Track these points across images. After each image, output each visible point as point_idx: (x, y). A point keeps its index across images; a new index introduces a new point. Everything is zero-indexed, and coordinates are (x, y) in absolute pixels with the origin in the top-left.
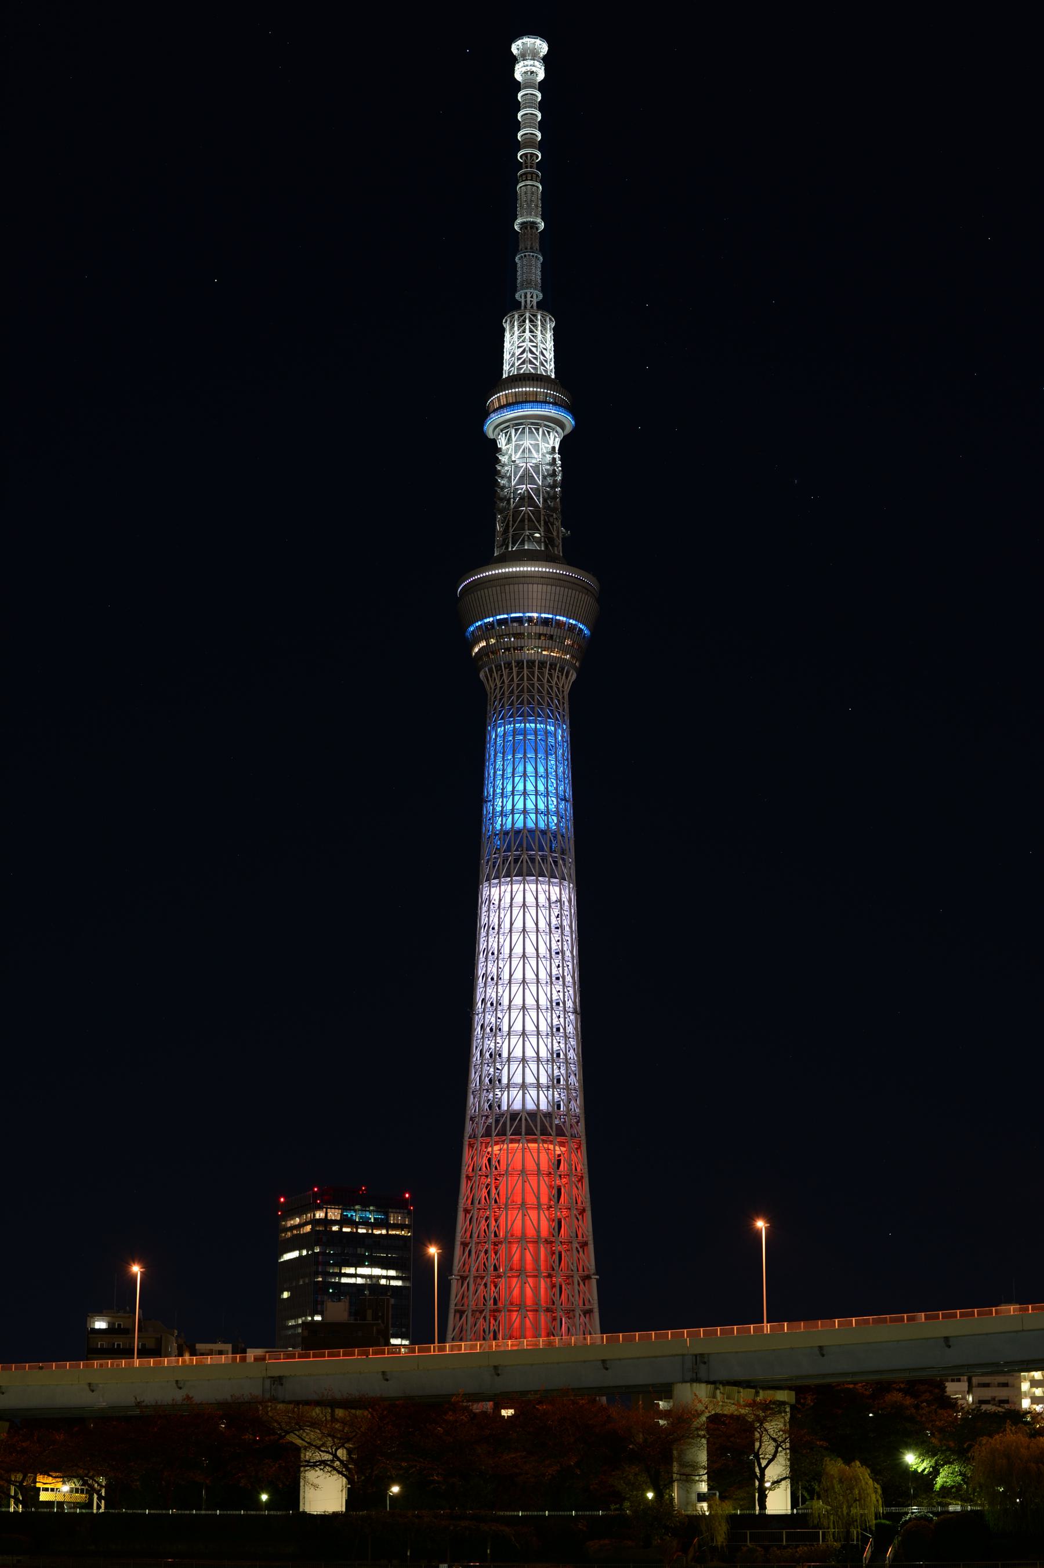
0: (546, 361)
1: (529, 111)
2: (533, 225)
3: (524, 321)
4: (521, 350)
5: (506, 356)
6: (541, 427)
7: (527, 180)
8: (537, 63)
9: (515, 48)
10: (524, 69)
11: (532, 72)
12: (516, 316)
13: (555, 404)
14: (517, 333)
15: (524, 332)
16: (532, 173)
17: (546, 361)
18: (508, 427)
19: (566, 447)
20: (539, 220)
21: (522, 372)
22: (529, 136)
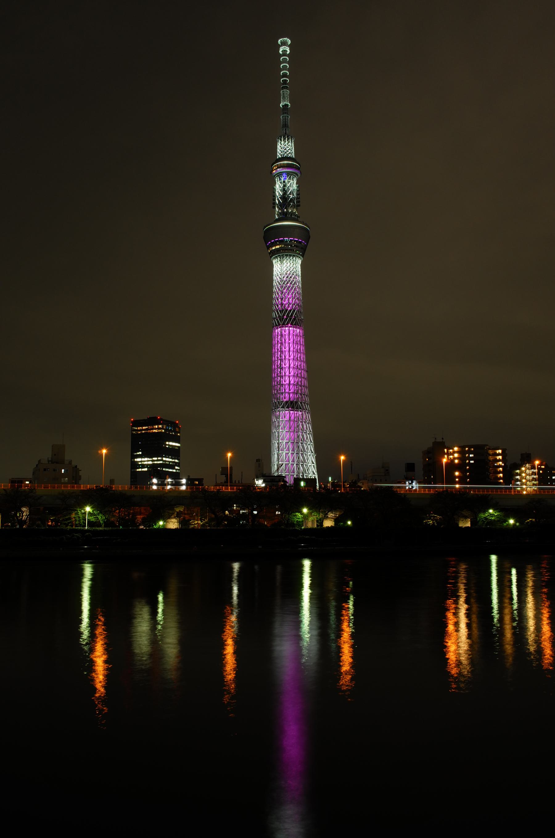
0: (292, 153)
2: (286, 105)
3: (285, 139)
5: (278, 151)
6: (292, 175)
7: (283, 89)
8: (287, 47)
9: (279, 41)
10: (283, 49)
11: (285, 50)
13: (296, 168)
14: (282, 142)
15: (285, 142)
16: (285, 87)
17: (292, 153)
20: (289, 104)
21: (284, 156)
22: (284, 73)
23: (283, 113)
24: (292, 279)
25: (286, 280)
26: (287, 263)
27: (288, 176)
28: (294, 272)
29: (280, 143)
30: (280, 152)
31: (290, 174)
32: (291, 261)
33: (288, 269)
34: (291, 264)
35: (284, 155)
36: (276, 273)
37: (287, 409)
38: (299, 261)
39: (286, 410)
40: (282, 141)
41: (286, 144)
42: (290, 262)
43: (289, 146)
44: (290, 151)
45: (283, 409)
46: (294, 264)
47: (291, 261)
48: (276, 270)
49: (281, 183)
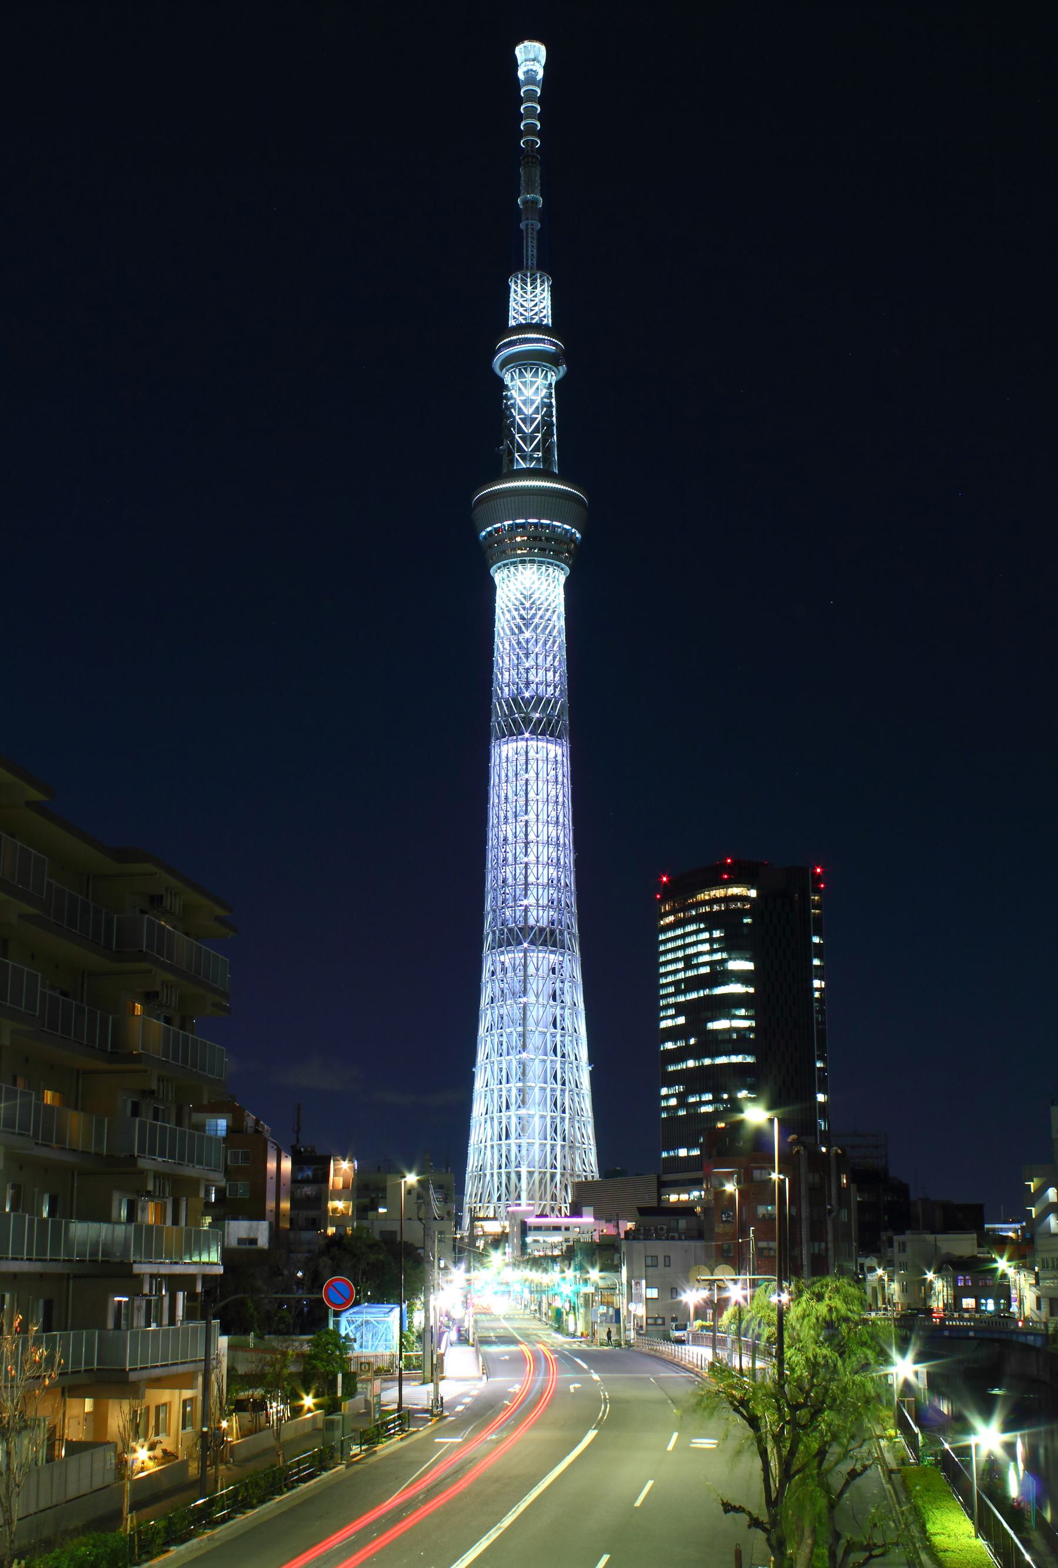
1: (530, 104)
2: (535, 202)
4: (533, 303)
12: (529, 274)
14: (529, 288)
15: (536, 288)
18: (526, 364)
19: (561, 388)
21: (534, 321)
23: (527, 219)
26: (540, 581)
27: (543, 370)
28: (556, 607)
29: (522, 288)
30: (521, 310)
31: (546, 367)
32: (550, 580)
33: (543, 598)
34: (549, 585)
35: (532, 319)
37: (540, 948)
38: (562, 579)
39: (540, 951)
40: (529, 284)
41: (539, 294)
42: (547, 580)
43: (544, 298)
44: (545, 312)
45: (533, 947)
46: (555, 587)
47: (550, 580)
48: (510, 594)
49: (524, 384)
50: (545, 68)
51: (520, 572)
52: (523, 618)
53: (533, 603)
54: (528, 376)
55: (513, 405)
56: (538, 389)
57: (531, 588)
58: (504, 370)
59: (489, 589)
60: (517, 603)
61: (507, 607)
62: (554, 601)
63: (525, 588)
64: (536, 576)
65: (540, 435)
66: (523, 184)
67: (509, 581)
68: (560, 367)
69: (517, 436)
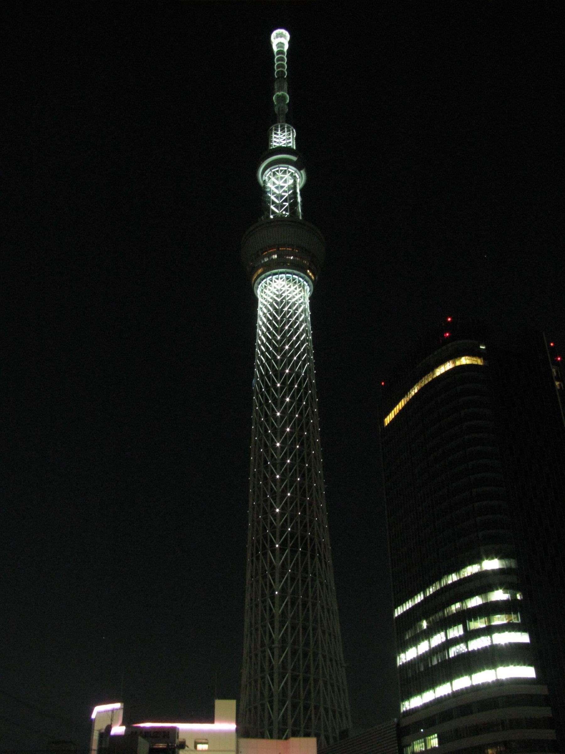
3: (284, 128)
12: (279, 126)
14: (279, 132)
24: (298, 313)
25: (289, 312)
28: (302, 303)
33: (291, 296)
34: (296, 289)
36: (266, 303)
40: (279, 131)
47: (297, 286)
49: (277, 179)
50: (290, 42)
51: (273, 281)
52: (275, 309)
53: (284, 298)
54: (280, 175)
55: (270, 192)
56: (286, 180)
57: (281, 290)
58: (264, 176)
59: (255, 301)
60: (271, 301)
61: (264, 305)
62: (300, 300)
63: (277, 290)
64: (284, 283)
65: (287, 204)
66: (276, 90)
67: (266, 289)
68: (302, 172)
69: (272, 207)
